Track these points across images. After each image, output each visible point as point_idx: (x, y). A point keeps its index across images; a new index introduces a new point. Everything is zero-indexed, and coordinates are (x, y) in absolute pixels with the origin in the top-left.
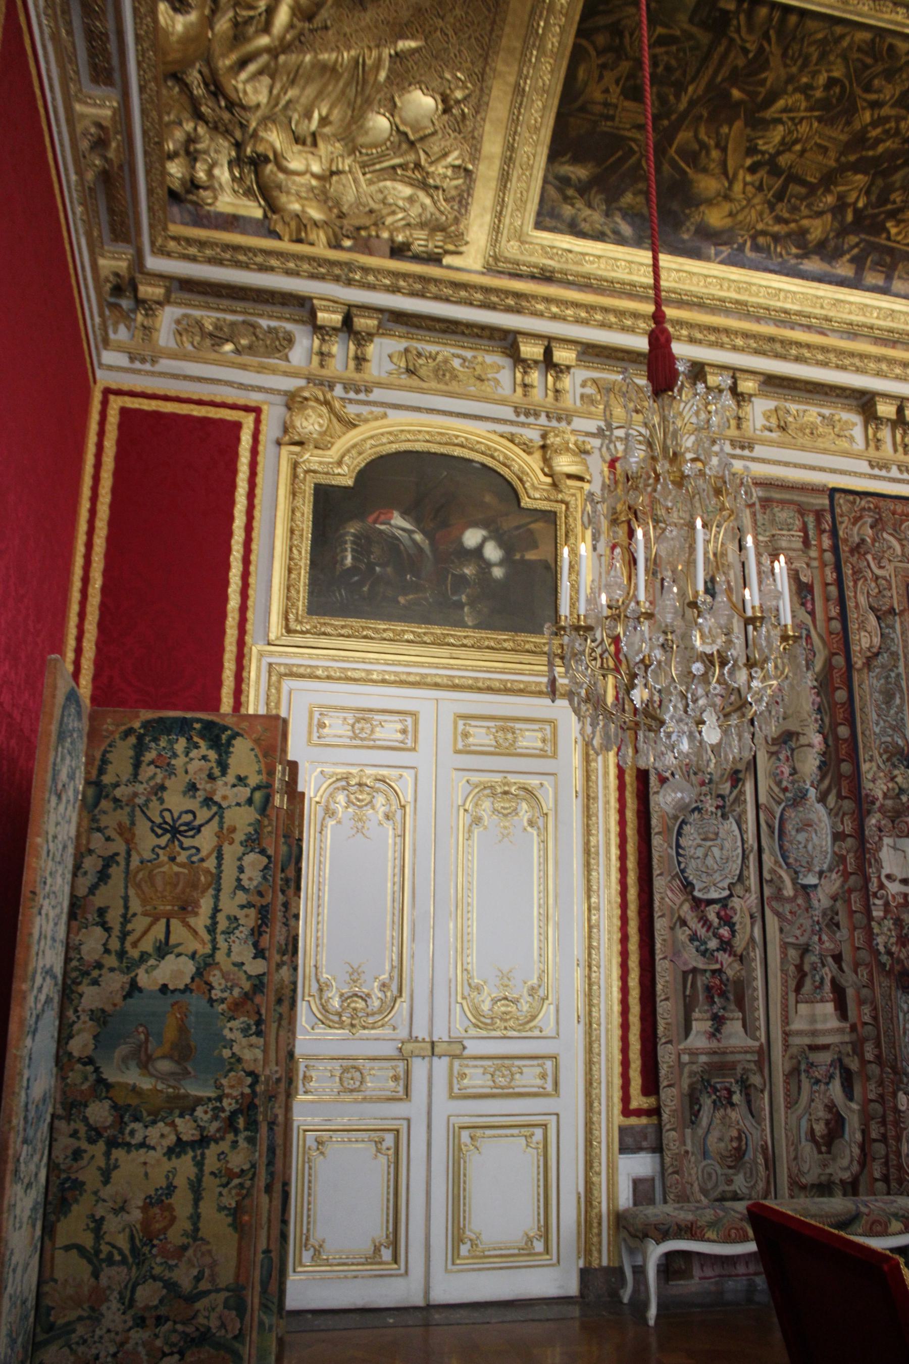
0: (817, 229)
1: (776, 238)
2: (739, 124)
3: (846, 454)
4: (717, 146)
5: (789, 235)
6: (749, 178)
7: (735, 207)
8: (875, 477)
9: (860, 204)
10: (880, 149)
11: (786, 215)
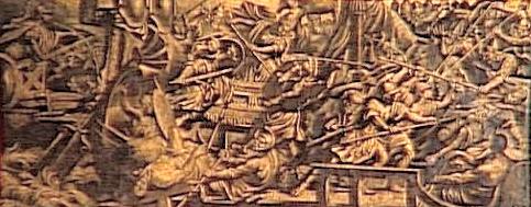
2: (158, 92)
4: (146, 114)
5: (241, 176)
6: (185, 135)
7: (180, 161)
10: (297, 89)
11: (232, 160)
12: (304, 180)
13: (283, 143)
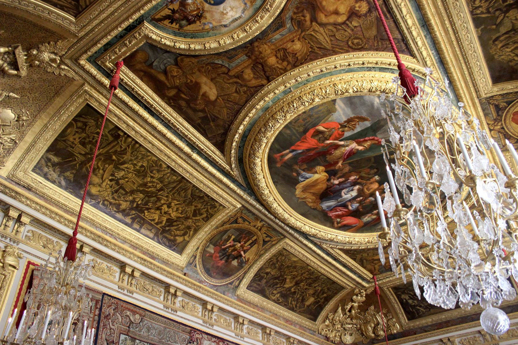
0: (124, 205)
1: (111, 203)
2: (112, 166)
3: (112, 282)
4: (103, 169)
5: (115, 204)
6: (109, 183)
7: (101, 189)
8: (119, 292)
9: (139, 203)
10: (150, 189)
11: (116, 198)
12: (131, 215)
13: (133, 202)
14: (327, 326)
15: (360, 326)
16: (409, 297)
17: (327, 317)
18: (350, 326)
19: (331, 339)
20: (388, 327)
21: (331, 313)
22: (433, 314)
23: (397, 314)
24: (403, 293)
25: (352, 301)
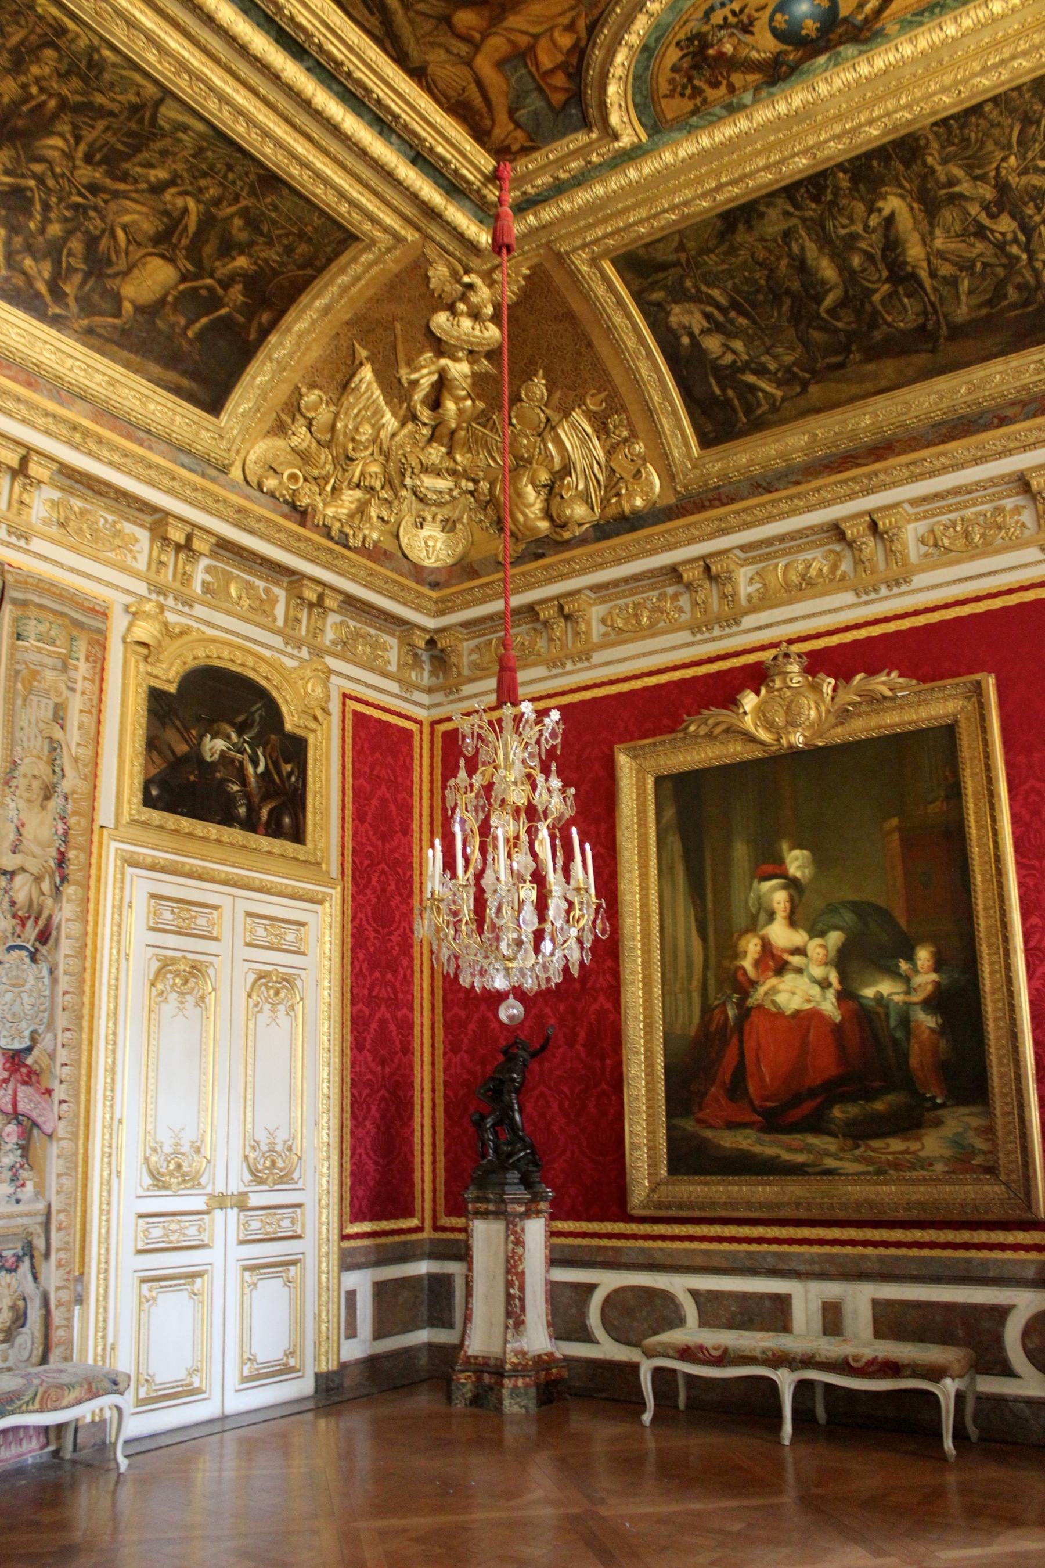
14: (303, 456)
15: (492, 484)
16: (708, 316)
17: (293, 407)
18: (443, 484)
19: (319, 520)
20: (612, 484)
21: (312, 386)
22: (817, 411)
23: (649, 412)
24: (679, 294)
25: (440, 347)
